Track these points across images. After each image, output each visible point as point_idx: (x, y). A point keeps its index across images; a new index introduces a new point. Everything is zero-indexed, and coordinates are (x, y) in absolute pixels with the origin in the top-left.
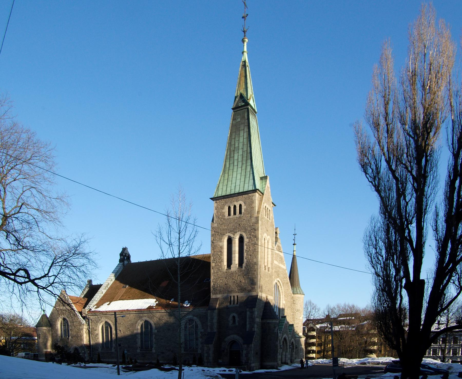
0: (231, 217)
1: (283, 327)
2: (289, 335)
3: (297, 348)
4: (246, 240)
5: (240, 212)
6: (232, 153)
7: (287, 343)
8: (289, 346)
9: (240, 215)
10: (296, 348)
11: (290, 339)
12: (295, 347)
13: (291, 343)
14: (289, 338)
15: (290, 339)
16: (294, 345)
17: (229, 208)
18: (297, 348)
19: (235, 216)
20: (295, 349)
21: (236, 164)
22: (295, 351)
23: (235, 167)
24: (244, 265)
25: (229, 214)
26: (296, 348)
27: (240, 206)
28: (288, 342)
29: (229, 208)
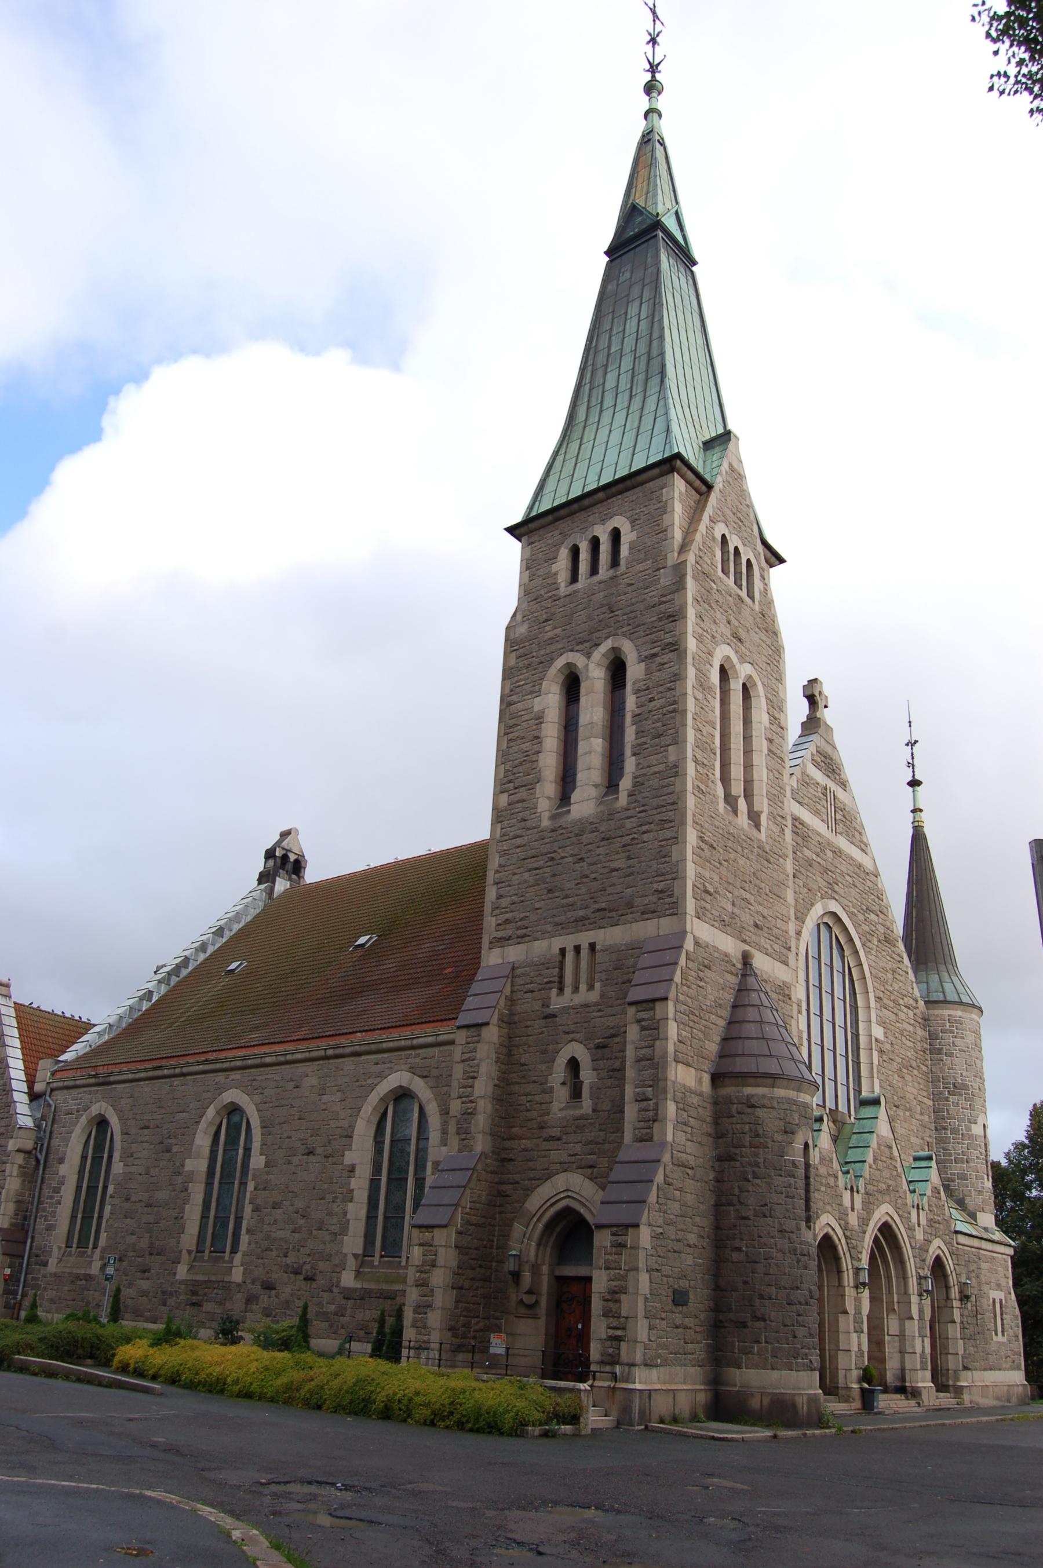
0: (579, 585)
1: (870, 1159)
2: (914, 1212)
3: (967, 1297)
4: (635, 671)
5: (615, 562)
6: (600, 373)
7: (901, 1262)
8: (920, 1278)
9: (611, 572)
10: (964, 1298)
11: (919, 1235)
12: (955, 1293)
13: (930, 1260)
14: (910, 1229)
15: (919, 1235)
16: (952, 1280)
17: (575, 551)
18: (967, 1297)
19: (596, 579)
20: (956, 1304)
21: (608, 401)
22: (957, 1316)
23: (607, 415)
24: (626, 784)
25: (574, 578)
26: (964, 1298)
27: (616, 535)
28: (908, 1252)
29: (575, 551)
